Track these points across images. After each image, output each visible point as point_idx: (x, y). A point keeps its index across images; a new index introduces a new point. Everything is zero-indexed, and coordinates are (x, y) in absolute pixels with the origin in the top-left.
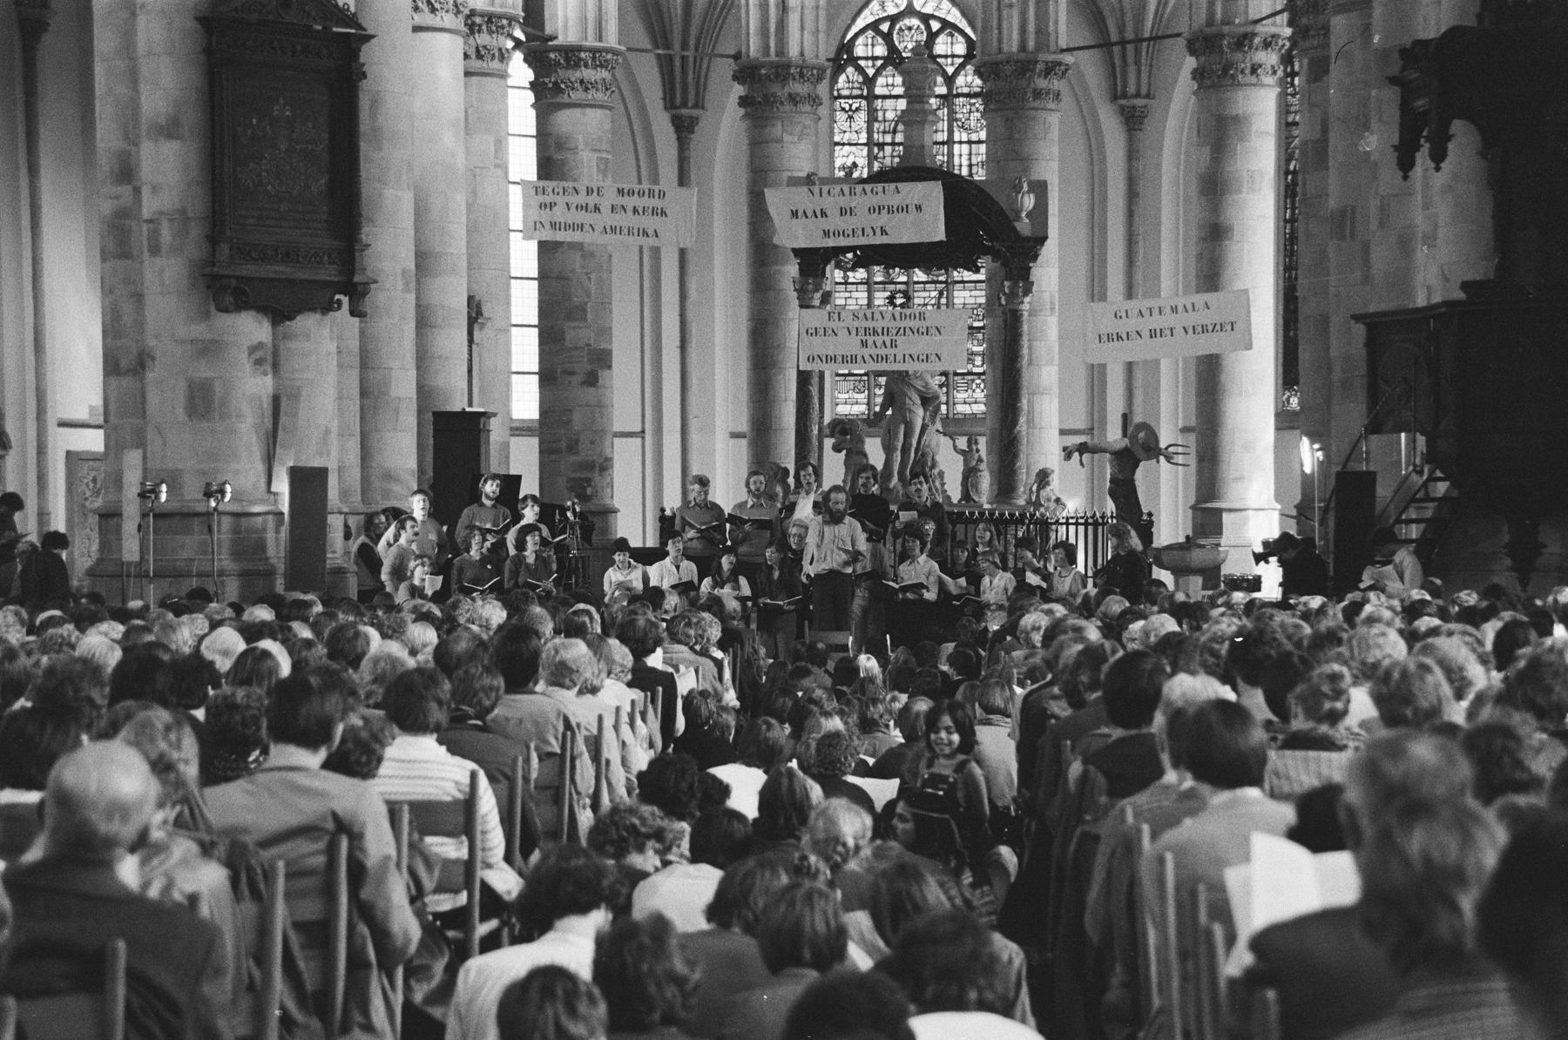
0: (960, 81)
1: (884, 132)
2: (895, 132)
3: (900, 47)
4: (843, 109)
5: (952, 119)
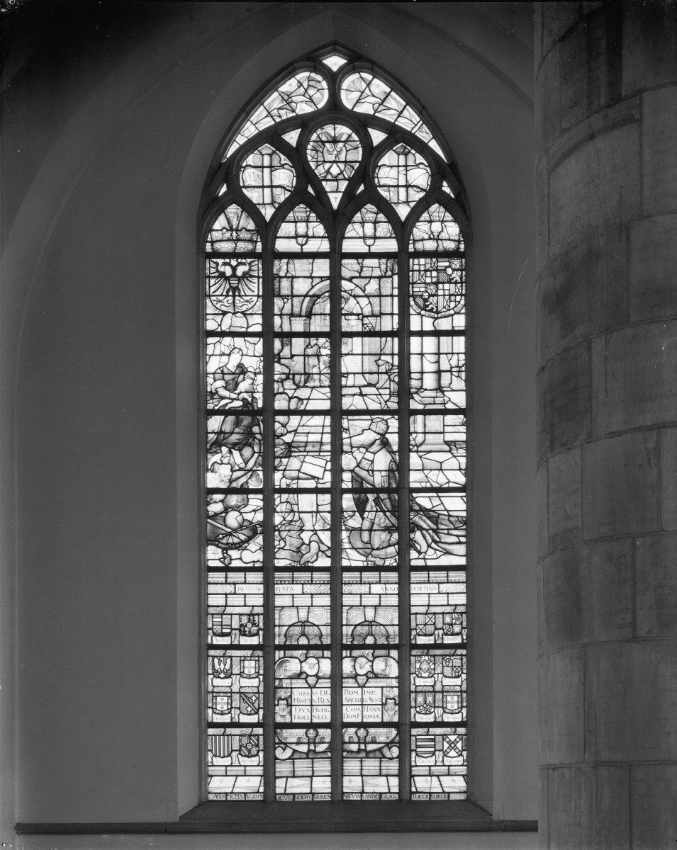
0: (420, 230)
1: (292, 315)
2: (309, 315)
3: (320, 171)
4: (222, 275)
5: (404, 296)
